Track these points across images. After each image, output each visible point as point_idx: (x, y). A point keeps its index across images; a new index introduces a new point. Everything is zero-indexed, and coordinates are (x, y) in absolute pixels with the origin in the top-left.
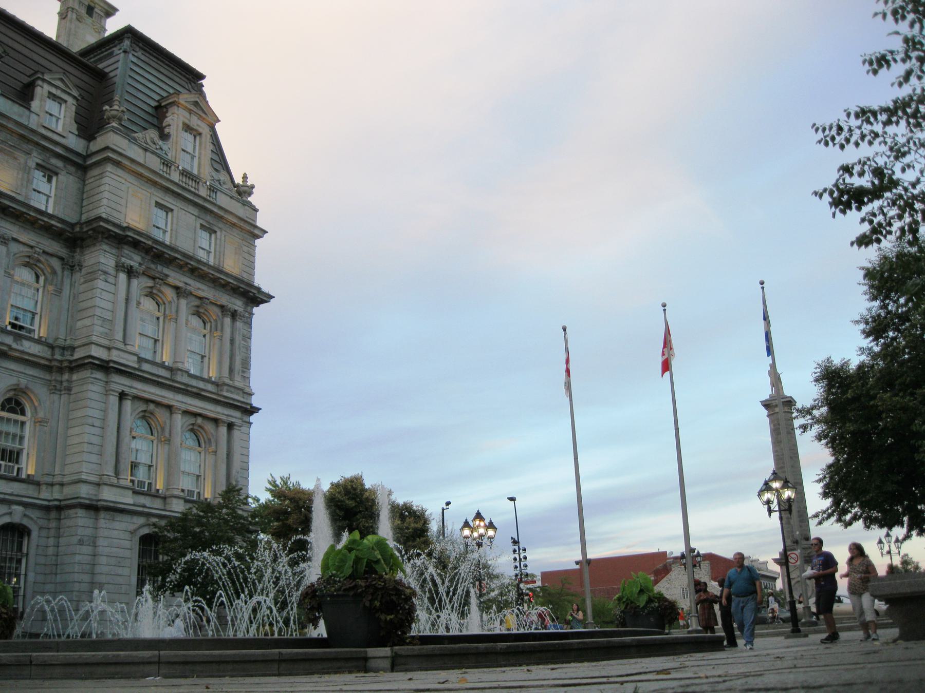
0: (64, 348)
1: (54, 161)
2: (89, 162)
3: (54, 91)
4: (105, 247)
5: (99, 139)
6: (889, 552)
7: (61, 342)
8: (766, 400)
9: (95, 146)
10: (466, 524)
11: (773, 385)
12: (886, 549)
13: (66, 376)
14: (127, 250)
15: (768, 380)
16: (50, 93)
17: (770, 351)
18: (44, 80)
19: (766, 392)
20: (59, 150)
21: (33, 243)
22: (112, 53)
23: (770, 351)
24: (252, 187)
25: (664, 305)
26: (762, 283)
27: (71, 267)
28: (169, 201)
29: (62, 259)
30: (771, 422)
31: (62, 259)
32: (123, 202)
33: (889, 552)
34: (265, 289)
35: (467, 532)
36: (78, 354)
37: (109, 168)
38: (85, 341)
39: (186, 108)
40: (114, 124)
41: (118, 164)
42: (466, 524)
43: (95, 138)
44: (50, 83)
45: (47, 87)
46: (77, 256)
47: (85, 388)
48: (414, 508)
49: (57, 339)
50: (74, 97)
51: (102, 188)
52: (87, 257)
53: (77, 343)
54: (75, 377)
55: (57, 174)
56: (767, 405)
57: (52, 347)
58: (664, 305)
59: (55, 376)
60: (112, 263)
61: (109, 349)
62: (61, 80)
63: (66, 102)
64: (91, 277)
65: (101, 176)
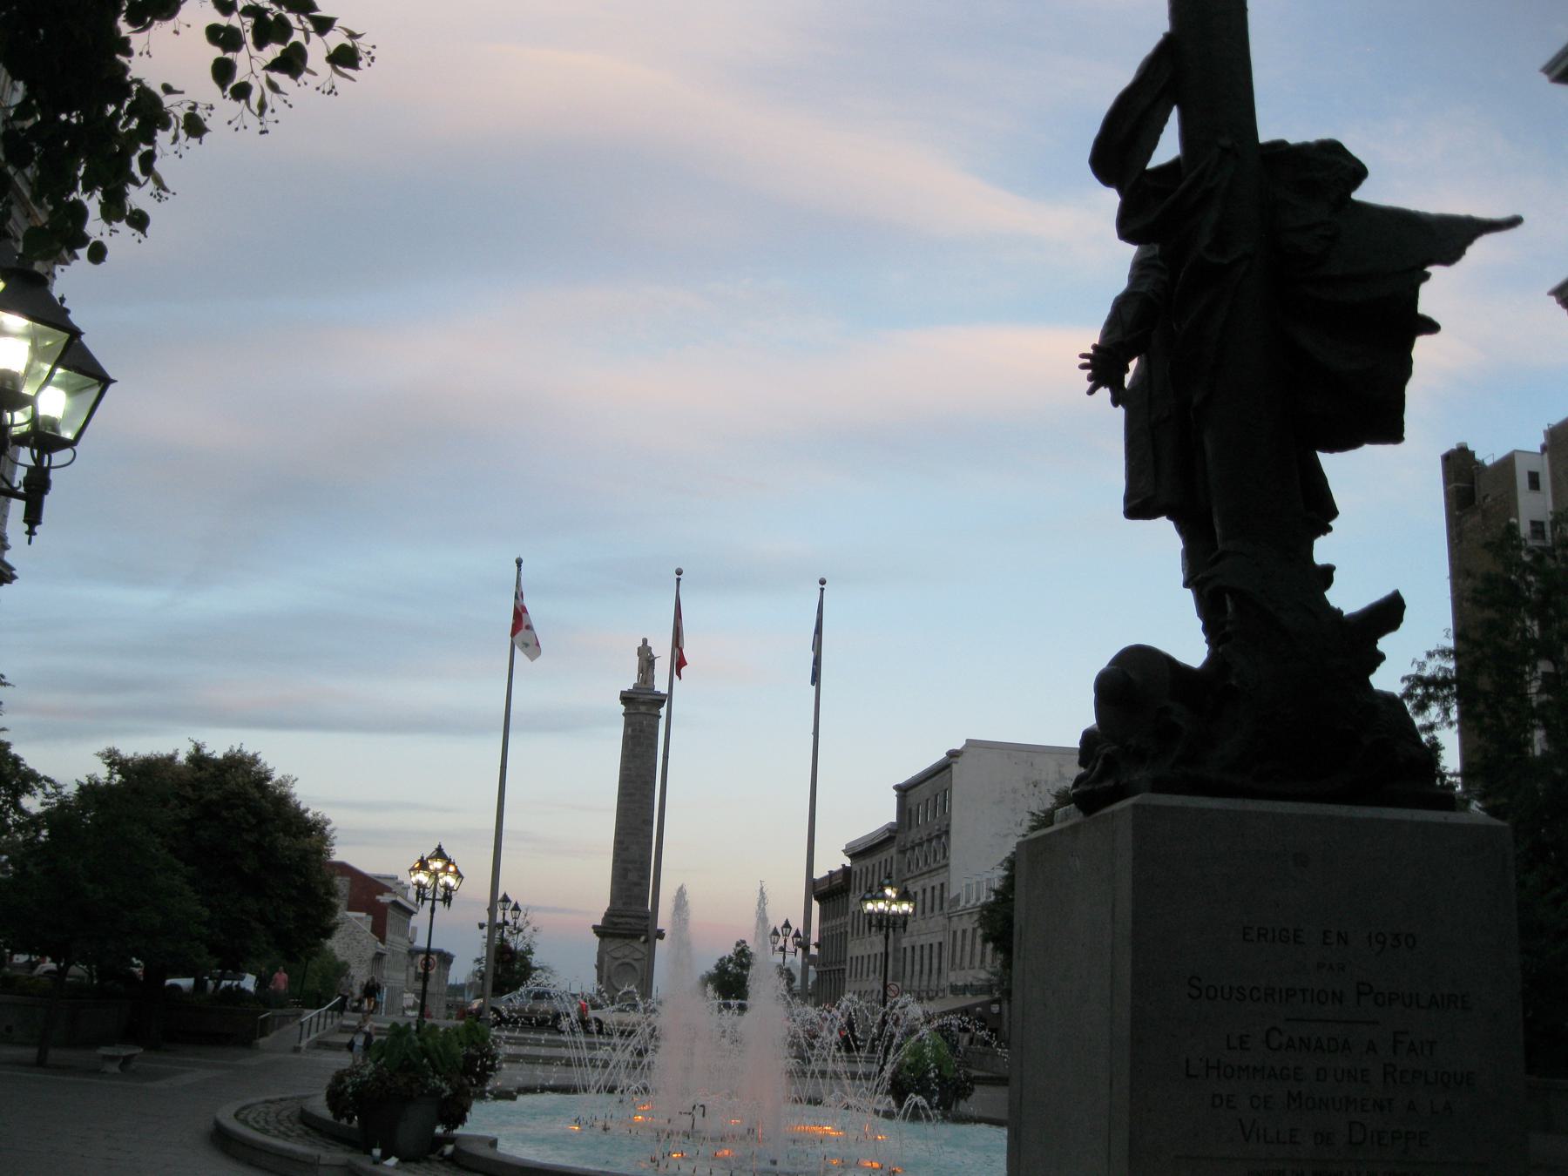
6: (783, 949)
8: (630, 692)
10: (423, 865)
11: (641, 670)
12: (781, 943)
15: (634, 661)
17: (816, 678)
19: (629, 681)
23: (816, 678)
25: (679, 572)
26: (823, 582)
30: (627, 725)
33: (783, 949)
35: (422, 877)
42: (423, 865)
48: (309, 815)
56: (626, 698)
58: (679, 572)
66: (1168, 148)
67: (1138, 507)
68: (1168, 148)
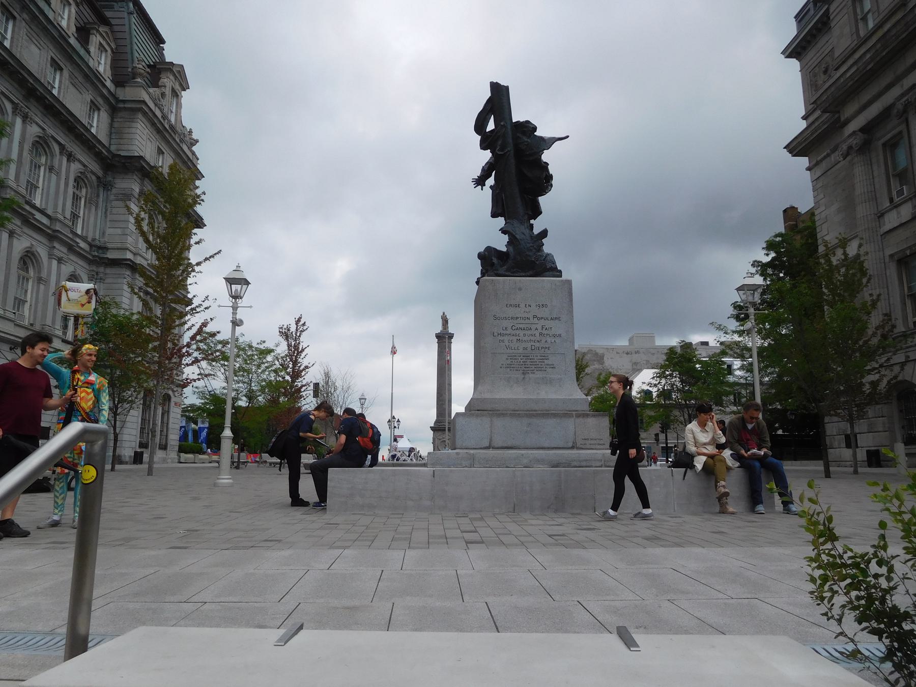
0: (99, 248)
1: (100, 100)
2: (121, 105)
3: (104, 43)
4: (135, 177)
5: (127, 89)
7: (97, 243)
9: (122, 94)
13: (101, 269)
14: (147, 182)
16: (100, 43)
18: (98, 31)
20: (105, 92)
21: (86, 163)
22: (112, 7)
24: (197, 141)
27: (105, 185)
28: (164, 148)
29: (98, 178)
31: (98, 178)
32: (144, 143)
34: (205, 222)
36: (111, 255)
37: (140, 116)
38: (119, 245)
39: (174, 75)
40: (139, 80)
41: (145, 114)
43: (124, 86)
44: (101, 35)
45: (99, 38)
46: (109, 178)
47: (120, 280)
49: (94, 240)
50: (112, 49)
51: (133, 130)
52: (117, 181)
53: (109, 246)
54: (108, 271)
55: (99, 110)
57: (91, 245)
59: (94, 268)
60: (137, 190)
61: (135, 254)
62: (106, 32)
63: (107, 51)
64: (126, 197)
65: (132, 120)
66: (491, 126)
67: (494, 215)
68: (491, 126)
